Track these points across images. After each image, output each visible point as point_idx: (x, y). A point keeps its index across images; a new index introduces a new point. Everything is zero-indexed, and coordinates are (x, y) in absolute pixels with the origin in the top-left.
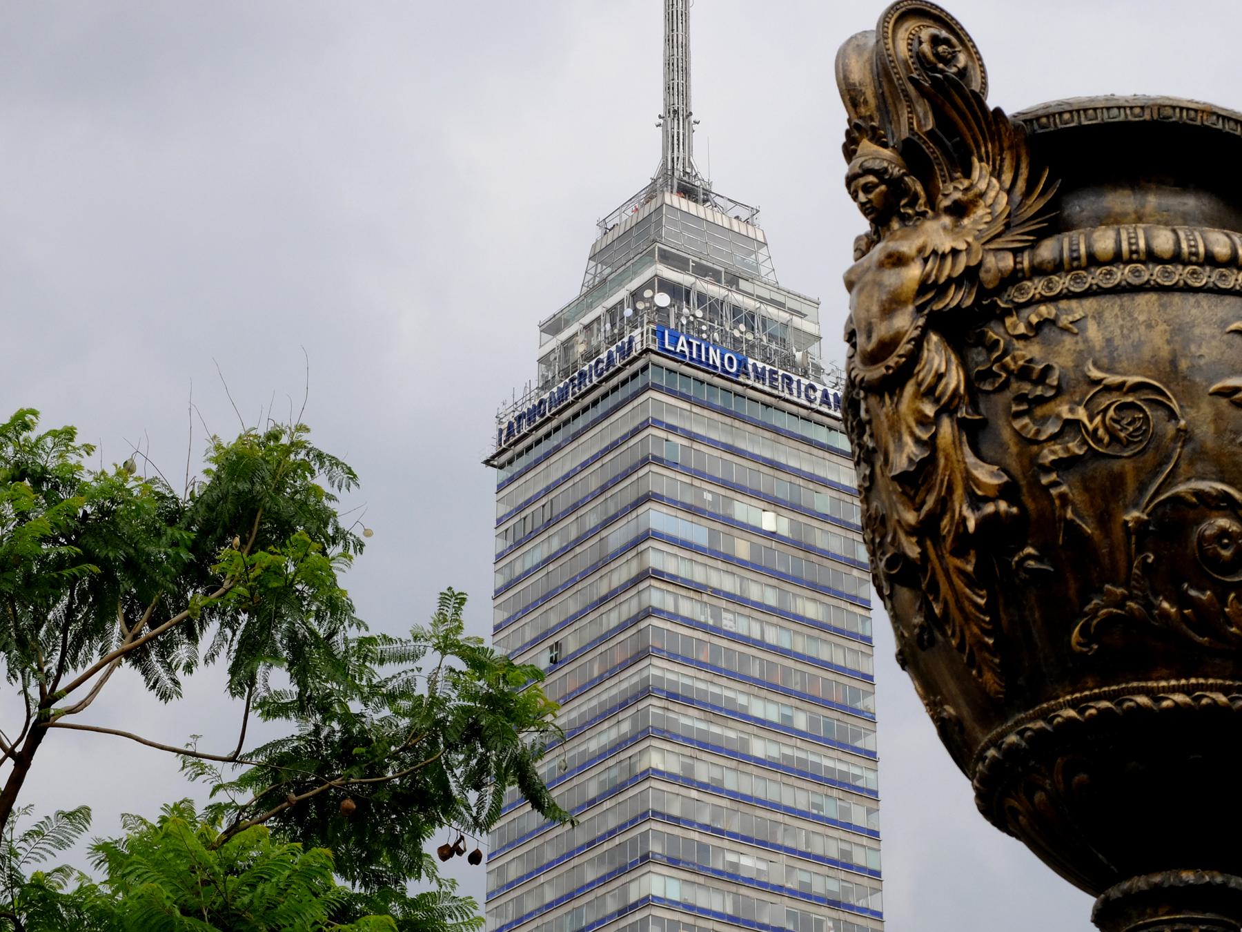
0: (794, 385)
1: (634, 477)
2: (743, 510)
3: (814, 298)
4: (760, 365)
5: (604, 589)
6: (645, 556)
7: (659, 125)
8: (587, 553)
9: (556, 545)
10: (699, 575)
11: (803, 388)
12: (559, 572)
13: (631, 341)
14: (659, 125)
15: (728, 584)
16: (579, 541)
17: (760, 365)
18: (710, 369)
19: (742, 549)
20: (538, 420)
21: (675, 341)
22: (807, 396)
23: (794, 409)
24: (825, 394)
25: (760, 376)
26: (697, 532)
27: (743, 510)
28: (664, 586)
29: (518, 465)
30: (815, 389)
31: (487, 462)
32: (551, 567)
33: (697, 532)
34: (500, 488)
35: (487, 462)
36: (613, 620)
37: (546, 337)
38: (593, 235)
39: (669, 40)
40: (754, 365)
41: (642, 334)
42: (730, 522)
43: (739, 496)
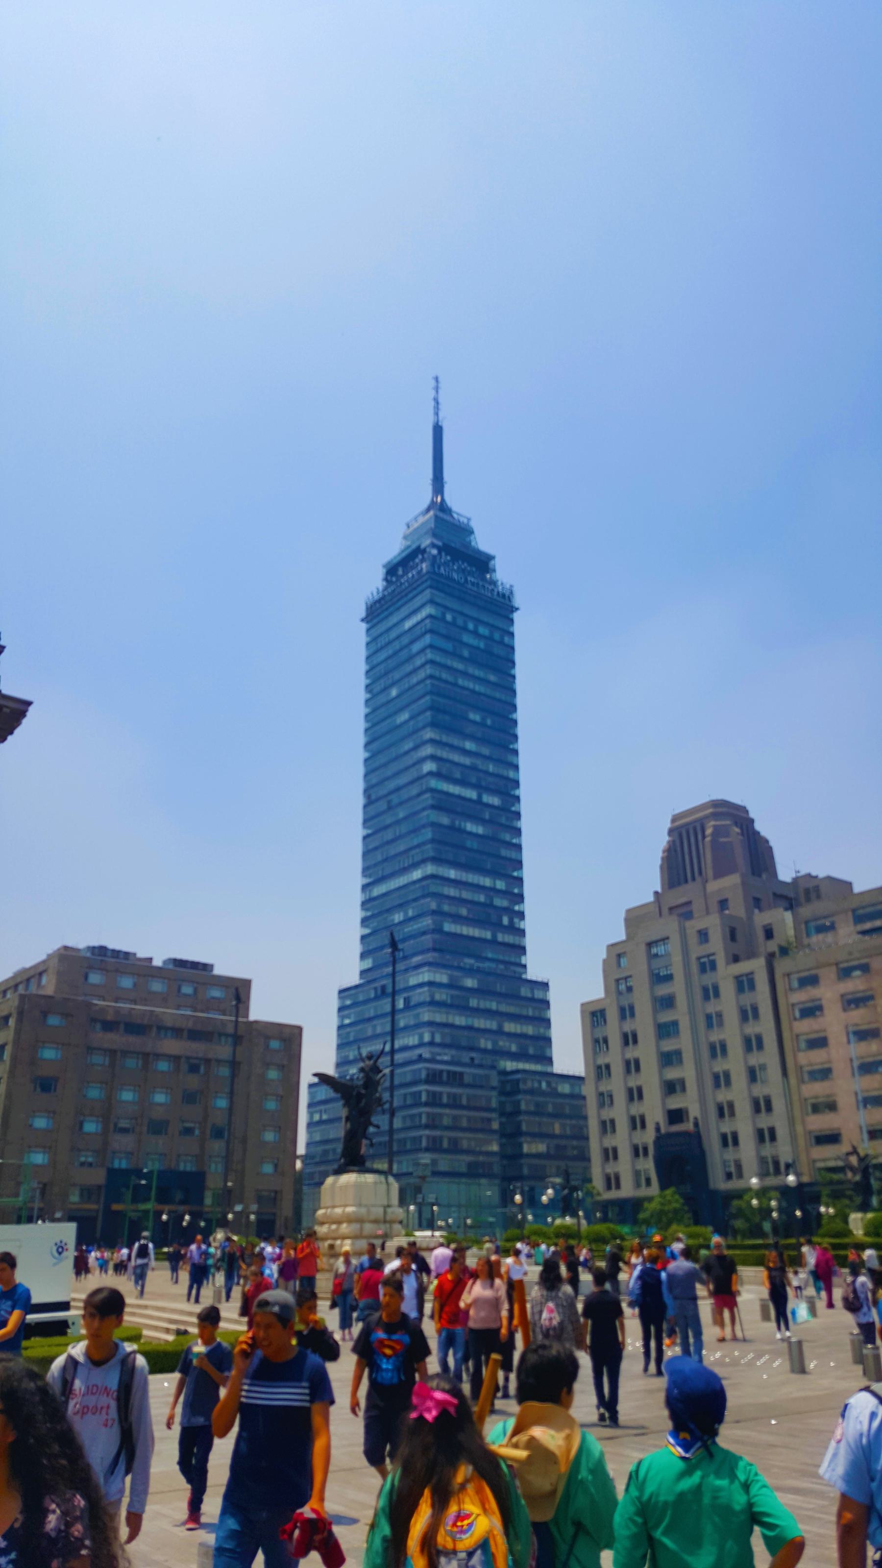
8: (404, 654)
9: (390, 652)
10: (449, 662)
12: (391, 663)
15: (460, 666)
16: (401, 649)
18: (453, 580)
19: (466, 653)
21: (439, 568)
24: (498, 593)
25: (473, 584)
26: (449, 646)
31: (363, 620)
33: (449, 646)
34: (368, 630)
35: (363, 620)
42: (461, 642)
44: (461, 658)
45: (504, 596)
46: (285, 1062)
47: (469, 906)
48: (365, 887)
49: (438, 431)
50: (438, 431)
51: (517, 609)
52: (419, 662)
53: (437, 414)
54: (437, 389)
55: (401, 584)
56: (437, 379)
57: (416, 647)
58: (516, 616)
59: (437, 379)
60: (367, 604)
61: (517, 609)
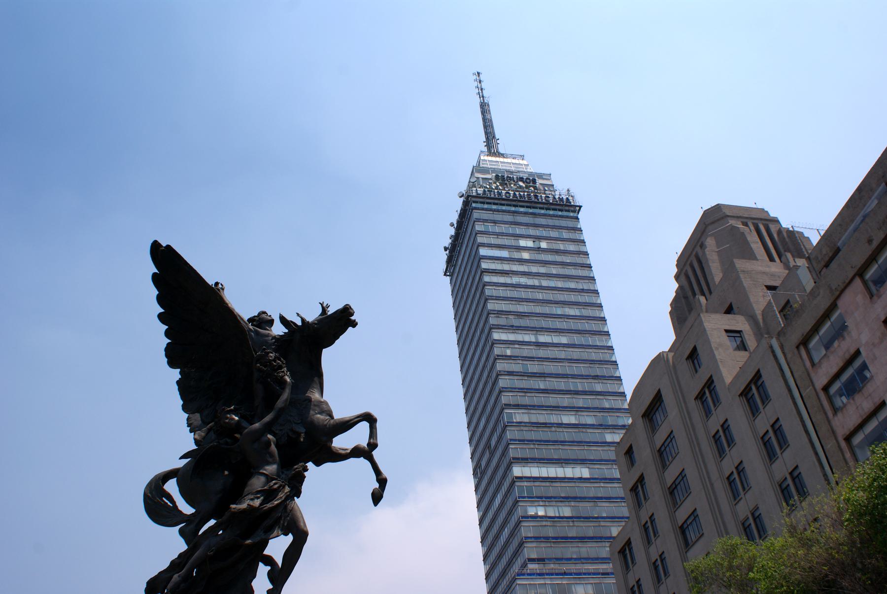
0: (539, 197)
2: (523, 243)
3: (549, 173)
4: (522, 193)
7: (485, 146)
10: (506, 267)
11: (543, 198)
14: (485, 146)
17: (522, 193)
19: (526, 255)
22: (546, 200)
23: (542, 206)
26: (505, 254)
27: (523, 243)
28: (490, 274)
30: (549, 197)
31: (445, 275)
35: (445, 275)
39: (484, 120)
40: (519, 194)
43: (520, 238)
44: (521, 261)
45: (561, 200)
47: (573, 504)
49: (484, 108)
50: (484, 108)
51: (580, 207)
58: (581, 216)
61: (580, 207)
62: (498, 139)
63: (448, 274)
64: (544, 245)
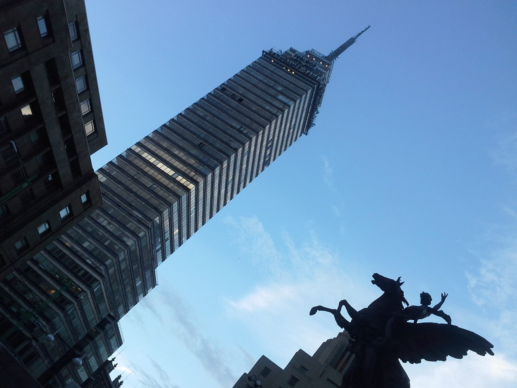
1: (295, 95)
5: (270, 101)
6: (285, 108)
7: (332, 51)
9: (265, 81)
12: (261, 85)
13: (317, 77)
14: (332, 51)
16: (272, 87)
20: (283, 60)
29: (265, 58)
31: (263, 51)
32: (261, 83)
35: (263, 51)
36: (268, 108)
37: (289, 50)
38: (310, 49)
41: (320, 79)
46: (75, 215)
48: (139, 144)
49: (351, 41)
50: (351, 41)
51: (306, 134)
52: (277, 104)
53: (357, 37)
54: (366, 29)
55: (300, 68)
56: (369, 27)
57: (281, 97)
59: (369, 27)
60: (272, 49)
61: (306, 134)
62: (336, 59)
63: (264, 54)
64: (291, 130)
